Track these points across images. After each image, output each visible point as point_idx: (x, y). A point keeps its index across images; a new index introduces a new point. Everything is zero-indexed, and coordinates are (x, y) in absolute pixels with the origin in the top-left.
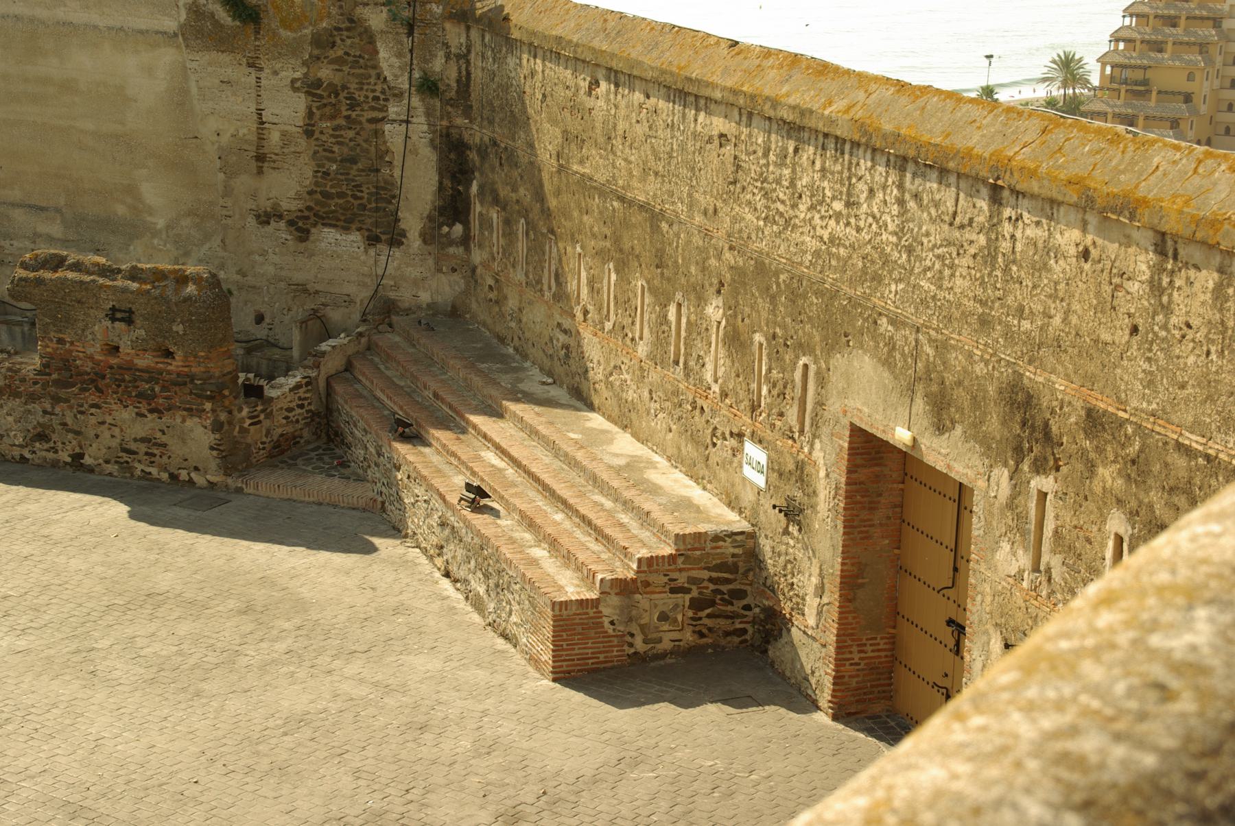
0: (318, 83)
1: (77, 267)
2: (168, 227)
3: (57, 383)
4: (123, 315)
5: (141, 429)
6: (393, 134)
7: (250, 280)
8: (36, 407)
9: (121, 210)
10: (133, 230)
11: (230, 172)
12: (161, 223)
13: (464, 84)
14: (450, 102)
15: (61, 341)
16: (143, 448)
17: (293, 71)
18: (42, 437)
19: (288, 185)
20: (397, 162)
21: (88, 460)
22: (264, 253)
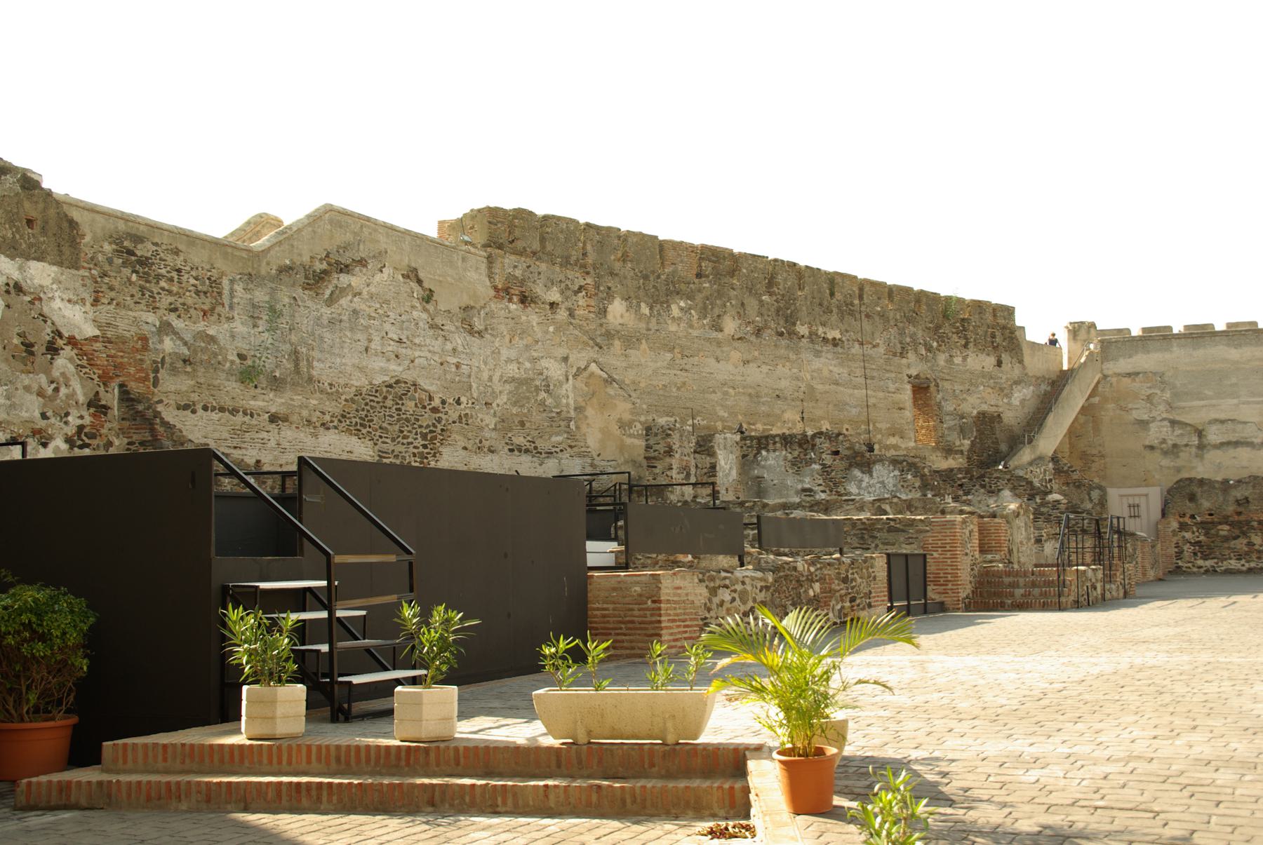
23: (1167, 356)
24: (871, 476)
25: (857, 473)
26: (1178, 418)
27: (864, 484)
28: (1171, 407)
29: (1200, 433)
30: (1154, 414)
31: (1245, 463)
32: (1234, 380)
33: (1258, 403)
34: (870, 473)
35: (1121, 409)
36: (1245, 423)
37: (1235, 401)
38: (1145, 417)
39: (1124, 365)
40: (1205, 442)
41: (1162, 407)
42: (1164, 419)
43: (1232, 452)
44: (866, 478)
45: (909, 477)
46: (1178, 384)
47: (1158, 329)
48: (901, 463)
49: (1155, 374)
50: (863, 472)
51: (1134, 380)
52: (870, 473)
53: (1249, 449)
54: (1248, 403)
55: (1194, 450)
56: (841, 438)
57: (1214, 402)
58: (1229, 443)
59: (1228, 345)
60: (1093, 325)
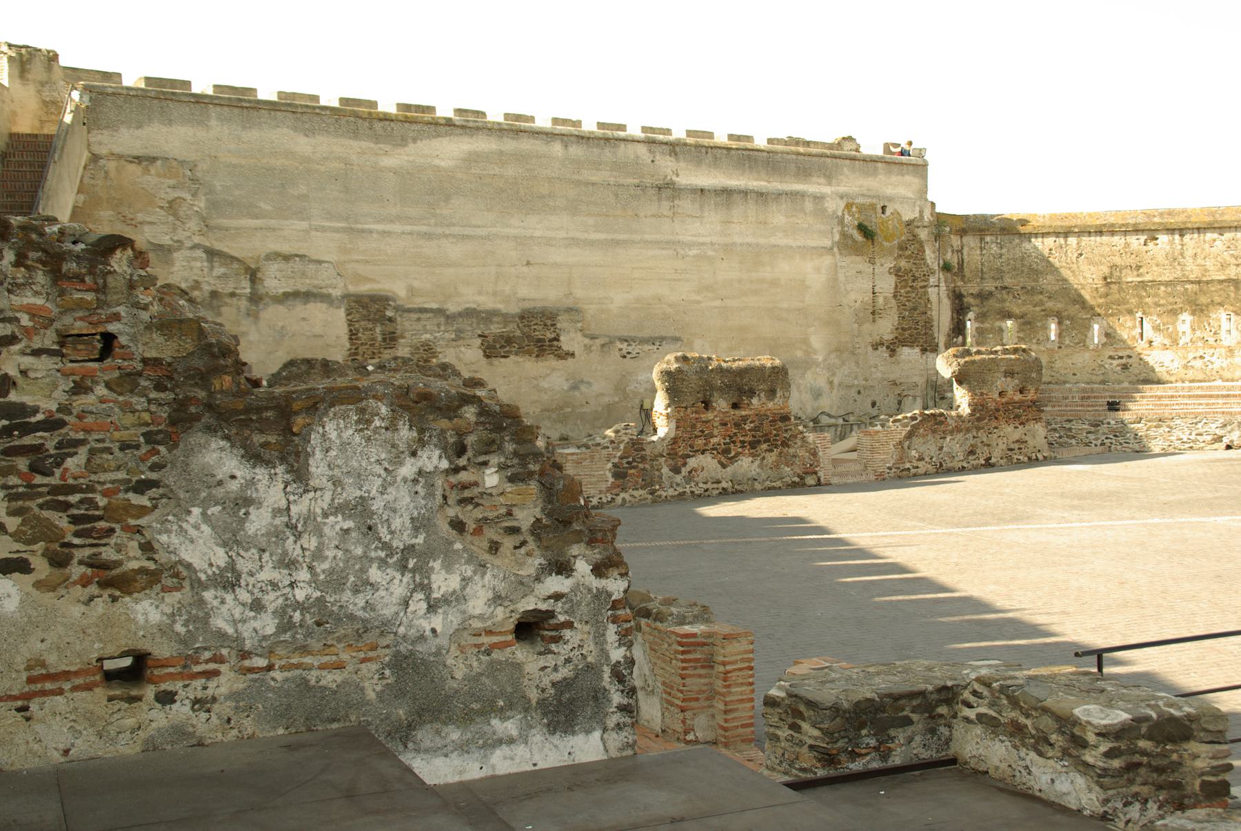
0: (899, 269)
1: (978, 352)
2: (825, 360)
3: (979, 419)
4: (1009, 374)
5: (1017, 434)
6: (932, 292)
7: (870, 383)
8: (970, 435)
9: (799, 354)
10: (807, 364)
11: (860, 323)
12: (820, 358)
13: (961, 264)
14: (955, 274)
15: (982, 394)
16: (1016, 446)
17: (889, 263)
18: (972, 452)
19: (886, 327)
20: (935, 306)
21: (993, 460)
22: (876, 366)
23: (201, 134)
24: (300, 475)
25: (220, 459)
26: (218, 246)
27: (258, 521)
28: (207, 227)
29: (253, 275)
30: (181, 235)
31: (318, 330)
32: (303, 189)
33: (337, 230)
34: (291, 457)
35: (124, 220)
36: (319, 262)
37: (304, 225)
38: (166, 240)
39: (128, 140)
40: (262, 291)
41: (193, 225)
42: (195, 247)
43: (300, 309)
44: (271, 489)
45: (491, 479)
46: (218, 185)
47: (173, 83)
48: (450, 408)
49: (182, 163)
50: (254, 457)
51: (147, 171)
52: (291, 457)
53: (324, 306)
54: (324, 229)
55: (244, 303)
56: (120, 262)
57: (273, 223)
58: (296, 295)
59: (295, 129)
60: (52, 57)
